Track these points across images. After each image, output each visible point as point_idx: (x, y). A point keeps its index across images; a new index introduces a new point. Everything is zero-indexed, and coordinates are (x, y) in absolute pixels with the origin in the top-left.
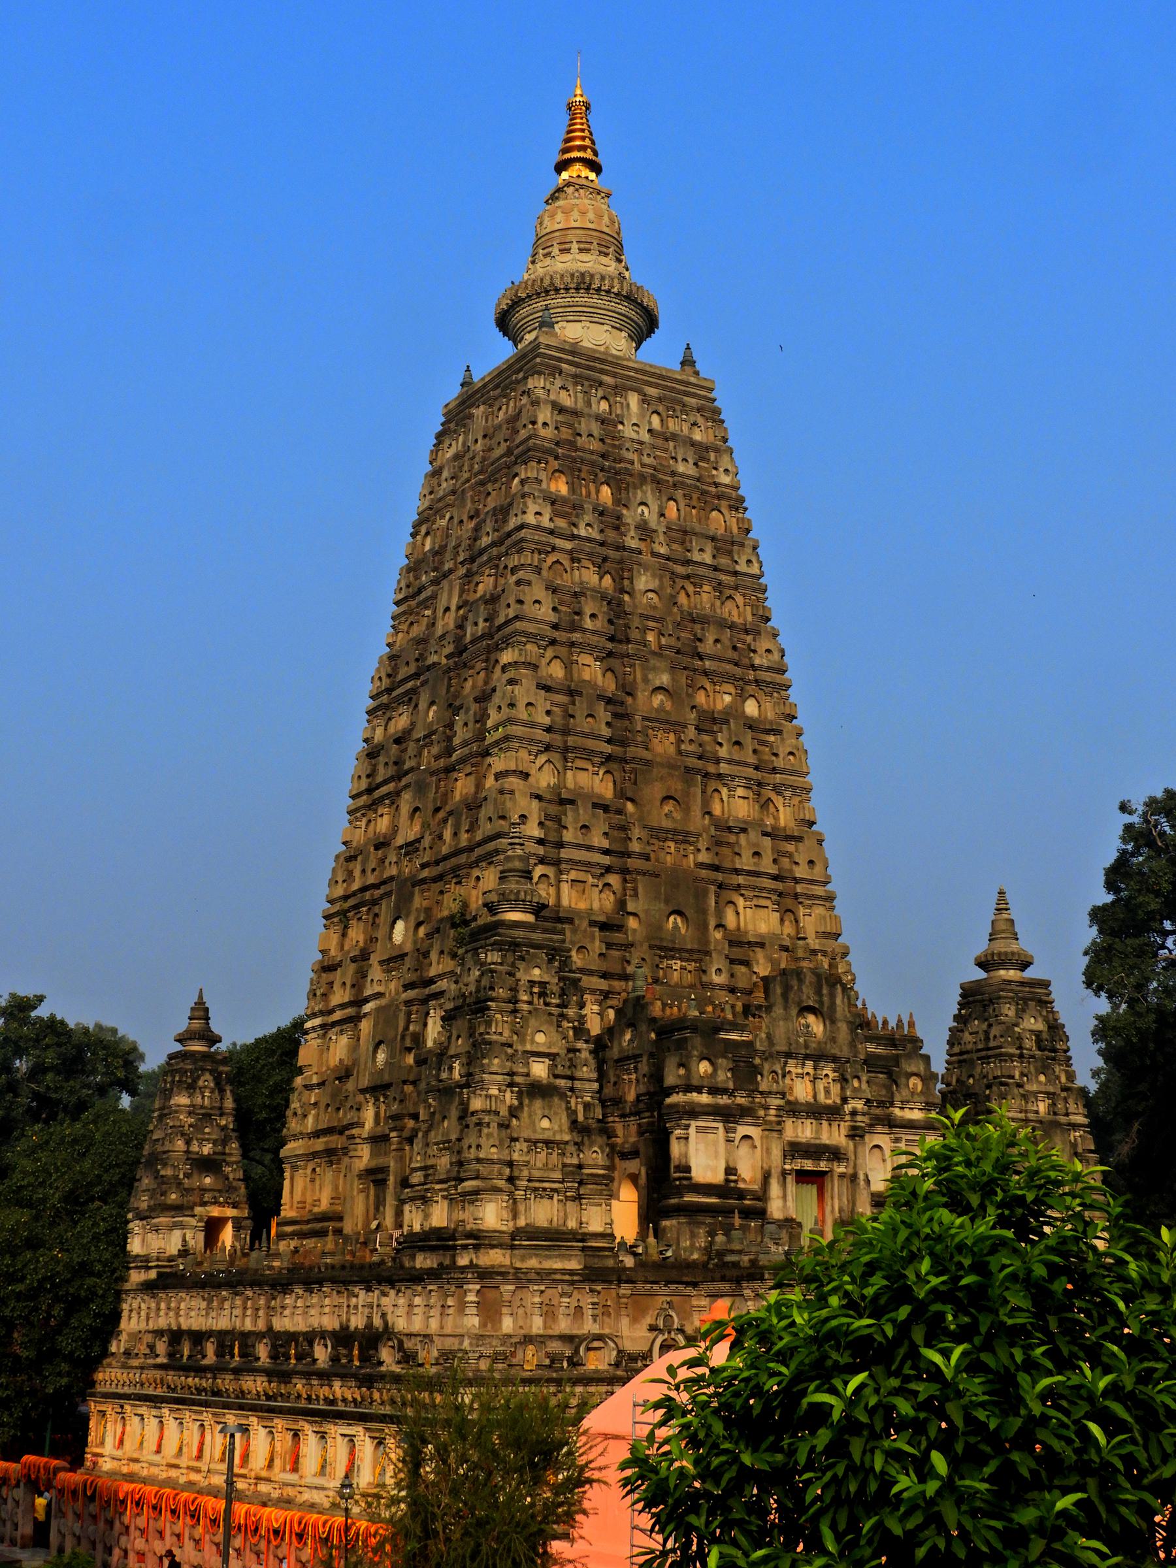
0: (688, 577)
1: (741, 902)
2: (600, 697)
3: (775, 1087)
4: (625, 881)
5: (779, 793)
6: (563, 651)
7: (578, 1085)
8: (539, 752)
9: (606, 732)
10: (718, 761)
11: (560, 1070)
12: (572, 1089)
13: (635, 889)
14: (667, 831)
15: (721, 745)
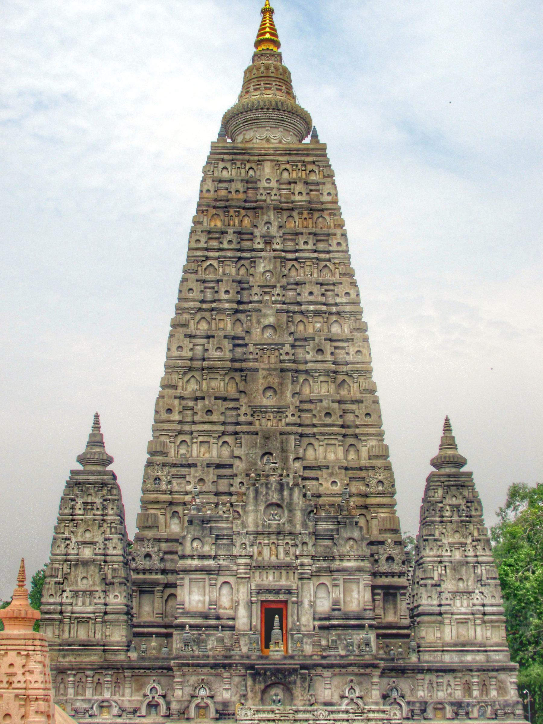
0: (296, 259)
1: (316, 444)
2: (225, 337)
3: (243, 553)
4: (236, 439)
5: (351, 376)
6: (207, 314)
7: (108, 558)
8: (185, 373)
9: (229, 355)
10: (306, 362)
11: (97, 551)
12: (105, 561)
13: (241, 443)
14: (266, 407)
15: (308, 353)
